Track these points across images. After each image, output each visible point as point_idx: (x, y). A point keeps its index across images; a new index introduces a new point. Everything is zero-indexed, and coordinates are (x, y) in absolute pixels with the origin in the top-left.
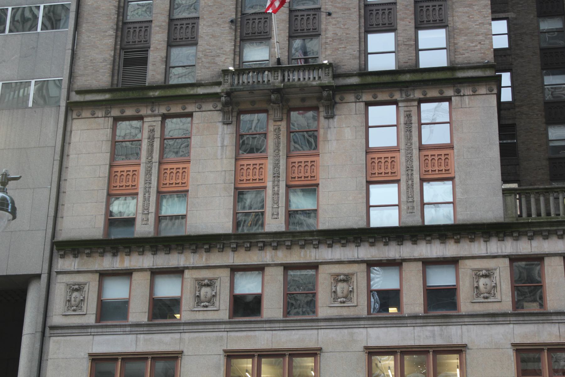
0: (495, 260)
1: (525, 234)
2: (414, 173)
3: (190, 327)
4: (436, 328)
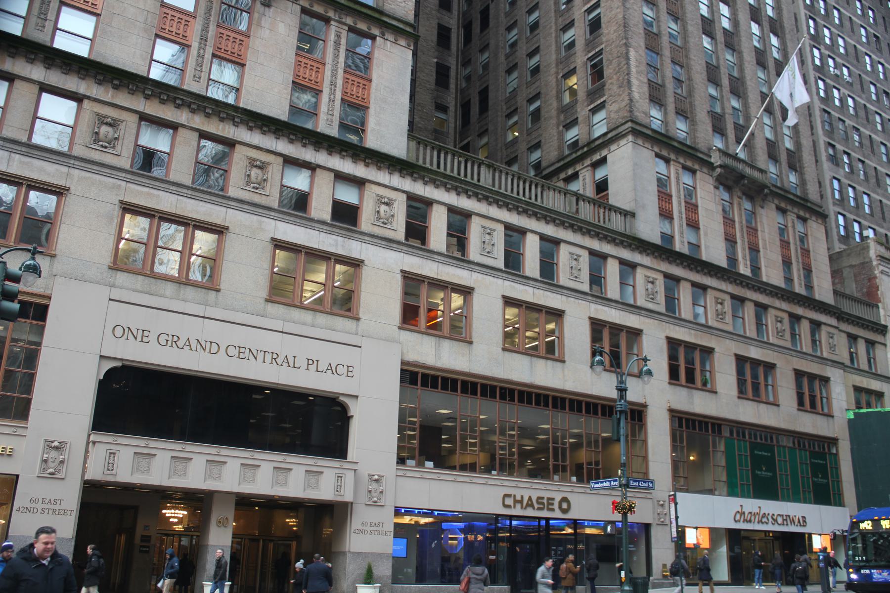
0: (396, 192)
1: (422, 178)
2: (337, 89)
3: (83, 164)
4: (340, 239)
